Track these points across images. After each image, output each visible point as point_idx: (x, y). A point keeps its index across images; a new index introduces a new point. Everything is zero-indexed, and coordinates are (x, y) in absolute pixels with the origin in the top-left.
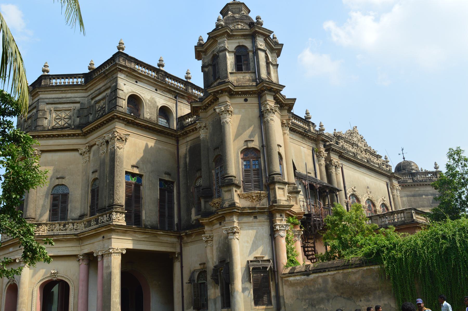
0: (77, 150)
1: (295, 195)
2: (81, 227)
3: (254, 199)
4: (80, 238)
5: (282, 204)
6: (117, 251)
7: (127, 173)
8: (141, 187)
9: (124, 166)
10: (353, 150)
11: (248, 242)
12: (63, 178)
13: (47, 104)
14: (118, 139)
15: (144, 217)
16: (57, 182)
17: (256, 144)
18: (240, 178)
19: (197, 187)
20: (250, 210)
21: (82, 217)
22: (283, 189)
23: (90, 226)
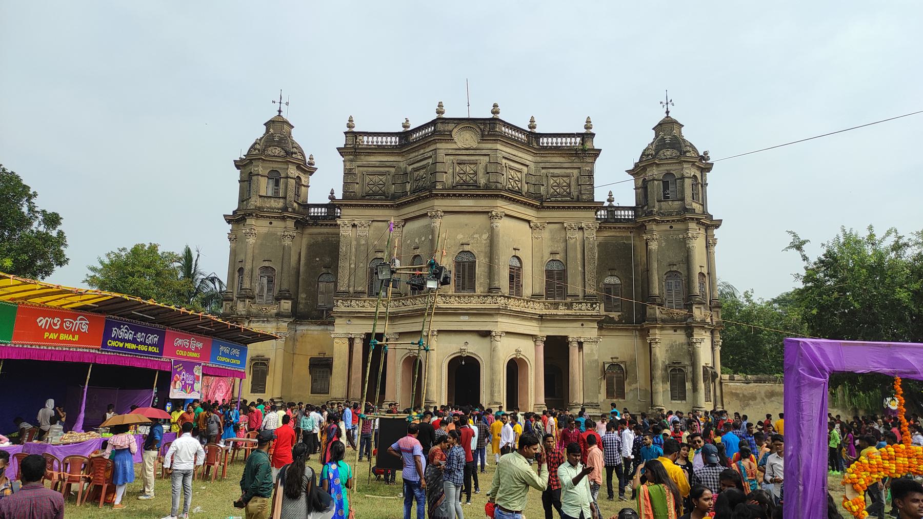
0: (529, 222)
2: (538, 308)
4: (542, 318)
17: (705, 271)
19: (606, 284)
21: (535, 297)
23: (557, 309)
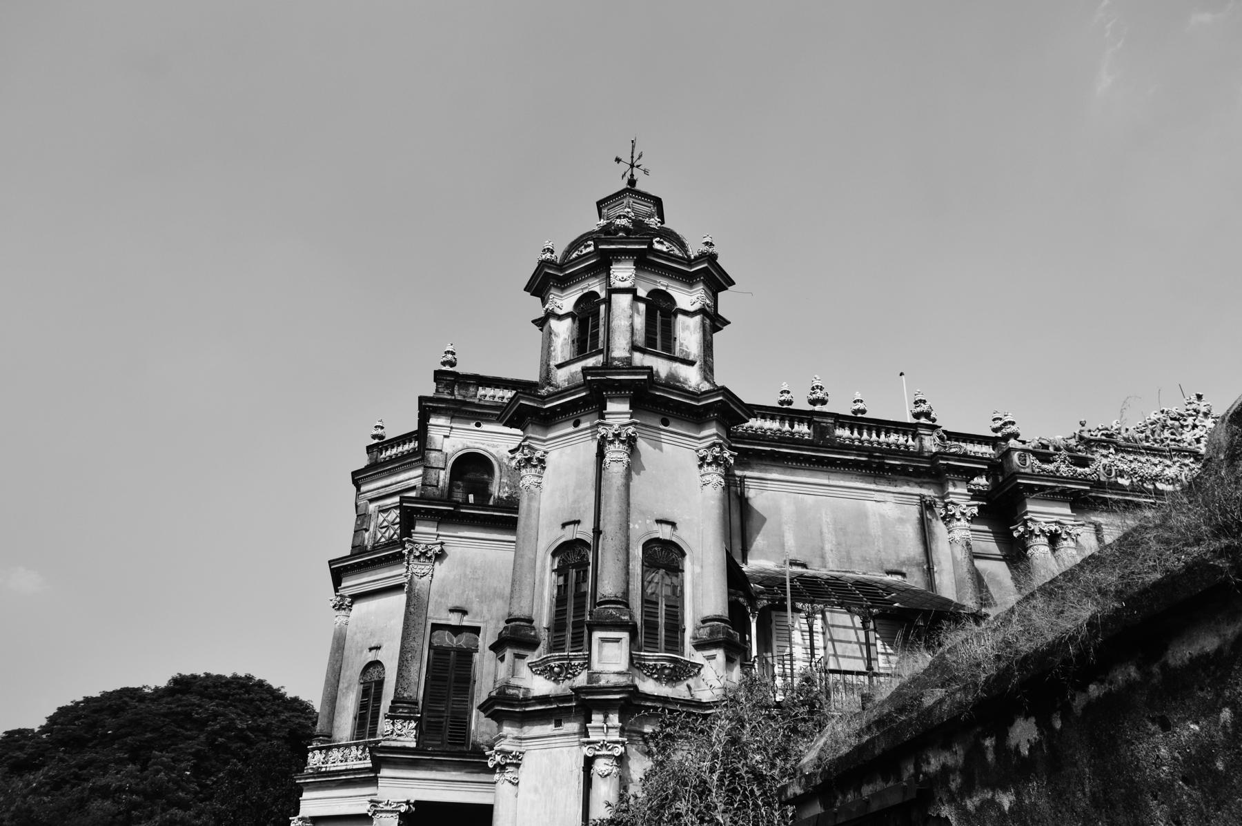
1: (713, 652)
3: (559, 674)
5: (603, 683)
6: (388, 808)
7: (435, 627)
8: (476, 656)
9: (430, 614)
10: (1170, 473)
11: (536, 790)
12: (378, 648)
13: (371, 501)
14: (416, 557)
15: (473, 727)
16: (371, 657)
18: (541, 621)
20: (541, 704)
22: (618, 640)
